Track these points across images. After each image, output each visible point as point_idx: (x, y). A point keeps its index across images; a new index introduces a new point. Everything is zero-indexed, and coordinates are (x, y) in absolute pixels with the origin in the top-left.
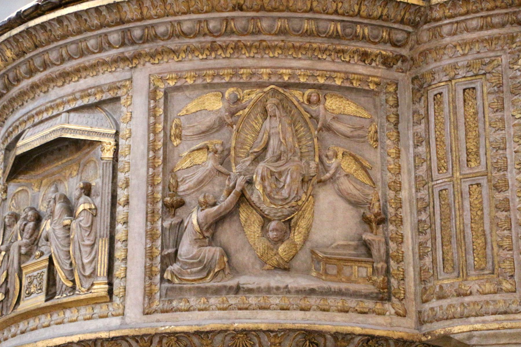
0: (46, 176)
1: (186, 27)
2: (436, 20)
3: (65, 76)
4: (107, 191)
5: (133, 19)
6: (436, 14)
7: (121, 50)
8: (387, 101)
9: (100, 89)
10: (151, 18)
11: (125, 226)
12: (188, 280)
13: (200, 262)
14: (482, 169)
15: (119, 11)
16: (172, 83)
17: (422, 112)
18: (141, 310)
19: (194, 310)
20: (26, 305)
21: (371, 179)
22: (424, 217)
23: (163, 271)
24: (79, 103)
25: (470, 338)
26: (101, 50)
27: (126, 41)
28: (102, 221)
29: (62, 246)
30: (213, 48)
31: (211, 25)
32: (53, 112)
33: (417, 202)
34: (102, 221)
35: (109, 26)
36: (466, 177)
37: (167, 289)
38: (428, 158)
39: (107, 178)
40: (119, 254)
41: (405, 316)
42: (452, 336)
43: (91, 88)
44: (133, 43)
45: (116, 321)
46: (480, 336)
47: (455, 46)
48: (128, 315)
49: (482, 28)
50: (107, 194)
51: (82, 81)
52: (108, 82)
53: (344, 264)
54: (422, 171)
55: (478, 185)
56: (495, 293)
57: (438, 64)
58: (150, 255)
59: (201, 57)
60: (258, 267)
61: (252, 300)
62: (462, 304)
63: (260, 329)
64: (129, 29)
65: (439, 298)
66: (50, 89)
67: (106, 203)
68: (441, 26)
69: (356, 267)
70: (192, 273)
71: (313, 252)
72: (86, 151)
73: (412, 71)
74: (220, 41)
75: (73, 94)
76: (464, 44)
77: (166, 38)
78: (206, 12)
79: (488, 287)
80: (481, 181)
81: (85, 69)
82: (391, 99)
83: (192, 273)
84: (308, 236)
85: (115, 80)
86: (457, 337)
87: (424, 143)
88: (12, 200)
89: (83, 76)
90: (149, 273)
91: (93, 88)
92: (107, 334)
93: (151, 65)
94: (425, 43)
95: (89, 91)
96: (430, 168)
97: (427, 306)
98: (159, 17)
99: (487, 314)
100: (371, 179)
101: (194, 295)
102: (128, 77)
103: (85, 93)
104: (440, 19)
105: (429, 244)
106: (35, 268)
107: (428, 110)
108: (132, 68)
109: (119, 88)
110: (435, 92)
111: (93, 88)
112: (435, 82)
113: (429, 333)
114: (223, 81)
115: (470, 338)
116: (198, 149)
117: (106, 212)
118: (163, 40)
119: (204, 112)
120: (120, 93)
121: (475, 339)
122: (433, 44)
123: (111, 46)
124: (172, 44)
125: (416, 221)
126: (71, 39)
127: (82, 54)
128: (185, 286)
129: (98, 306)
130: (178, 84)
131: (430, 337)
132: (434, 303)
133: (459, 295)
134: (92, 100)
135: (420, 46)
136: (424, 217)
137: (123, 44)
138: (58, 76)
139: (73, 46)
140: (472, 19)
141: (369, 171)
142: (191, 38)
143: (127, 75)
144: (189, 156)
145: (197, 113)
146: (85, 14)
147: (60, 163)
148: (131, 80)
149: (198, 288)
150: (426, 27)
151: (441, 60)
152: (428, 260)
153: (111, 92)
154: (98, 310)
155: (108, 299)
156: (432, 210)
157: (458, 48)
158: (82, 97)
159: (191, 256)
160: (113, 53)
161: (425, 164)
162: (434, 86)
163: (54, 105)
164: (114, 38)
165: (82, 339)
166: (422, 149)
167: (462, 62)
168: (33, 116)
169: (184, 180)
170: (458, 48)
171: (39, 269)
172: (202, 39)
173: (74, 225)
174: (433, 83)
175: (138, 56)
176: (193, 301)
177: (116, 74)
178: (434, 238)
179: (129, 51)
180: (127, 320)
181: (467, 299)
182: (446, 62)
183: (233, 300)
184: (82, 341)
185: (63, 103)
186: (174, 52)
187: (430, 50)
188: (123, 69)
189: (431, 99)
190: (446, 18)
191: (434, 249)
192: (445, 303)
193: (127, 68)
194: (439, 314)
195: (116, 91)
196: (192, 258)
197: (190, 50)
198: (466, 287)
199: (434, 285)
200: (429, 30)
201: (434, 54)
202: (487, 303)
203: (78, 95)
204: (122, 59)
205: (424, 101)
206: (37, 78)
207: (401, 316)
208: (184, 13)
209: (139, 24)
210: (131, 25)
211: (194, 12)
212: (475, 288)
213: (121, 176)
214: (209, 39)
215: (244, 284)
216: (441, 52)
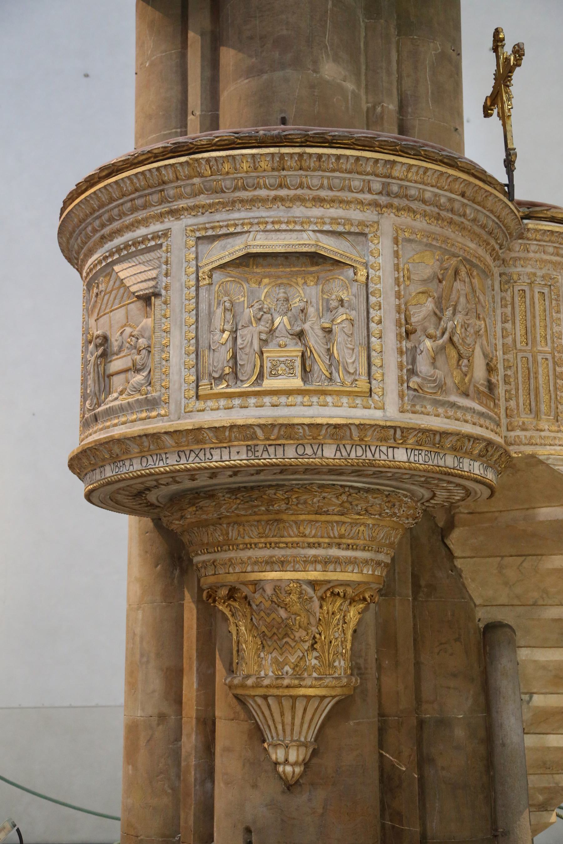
0: (269, 276)
1: (427, 195)
2: (528, 239)
3: (319, 201)
4: (362, 308)
5: (381, 174)
6: (530, 235)
7: (376, 197)
9: (349, 221)
10: (411, 181)
11: (379, 340)
12: (427, 392)
13: (435, 381)
14: (548, 349)
15: (392, 168)
17: (509, 299)
18: (398, 409)
19: (432, 415)
20: (269, 384)
22: (509, 373)
23: (408, 382)
24: (326, 228)
25: (548, 459)
26: (362, 191)
27: (384, 192)
28: (360, 332)
29: (323, 343)
30: (438, 217)
31: (443, 200)
32: (294, 226)
33: (504, 361)
34: (360, 332)
35: (377, 176)
36: (540, 352)
37: (415, 396)
38: (514, 333)
39: (362, 298)
40: (376, 360)
42: (537, 456)
43: (341, 218)
44: (388, 195)
45: (378, 414)
46: (554, 459)
47: (536, 261)
48: (388, 410)
49: (552, 254)
50: (362, 311)
51: (332, 210)
52: (358, 218)
54: (509, 340)
55: (547, 359)
56: (557, 432)
57: (523, 269)
58: (401, 367)
59: (428, 221)
60: (455, 390)
61: (459, 414)
62: (540, 436)
64: (389, 184)
65: (523, 430)
66: (294, 206)
67: (363, 318)
68: (529, 244)
70: (430, 387)
71: (475, 386)
72: (328, 268)
73: (500, 268)
74: (443, 214)
75: (322, 218)
76: (542, 261)
77: (411, 199)
78: (445, 190)
79: (554, 428)
80: (548, 357)
81: (341, 202)
83: (430, 387)
85: (364, 219)
86: (541, 458)
87: (510, 322)
88: (219, 286)
89: (335, 207)
90: (401, 381)
91: (343, 219)
92: (384, 423)
93: (394, 216)
94: (515, 252)
95: (339, 220)
96: (514, 341)
97: (512, 434)
98: (416, 182)
99: (556, 445)
101: (430, 404)
102: (376, 220)
103: (334, 220)
104: (531, 240)
105: (513, 392)
106: (288, 354)
107: (513, 300)
108: (379, 214)
109: (368, 227)
110: (519, 289)
111: (343, 219)
112: (520, 281)
113: (520, 452)
114: (438, 245)
115: (548, 459)
116: (423, 293)
117: (363, 325)
118: (408, 200)
119: (423, 264)
120: (367, 230)
121: (551, 460)
122: (522, 255)
123: (370, 191)
124: (414, 205)
125: (503, 375)
126: (337, 174)
127: (342, 189)
128: (428, 396)
129: (359, 398)
130: (411, 237)
131: (520, 455)
132: (518, 433)
133: (537, 430)
134: (340, 229)
135: (511, 253)
136: (509, 373)
137: (380, 193)
138: (311, 199)
139: (337, 181)
140: (549, 246)
142: (426, 205)
143: (375, 218)
144: (416, 296)
145: (420, 264)
146: (365, 161)
147: (288, 270)
148: (378, 223)
149: (435, 399)
150: (520, 241)
151: (526, 267)
152: (512, 403)
153: (360, 228)
154: (358, 401)
155: (369, 394)
156: (516, 369)
157: (538, 263)
158: (331, 224)
159: (430, 374)
160: (368, 197)
161: (511, 336)
162: (519, 284)
163: (298, 221)
164: (376, 186)
165: (362, 422)
166: (509, 326)
167: (540, 273)
168: (267, 223)
169: (414, 314)
170: (538, 263)
171: (287, 356)
172: (433, 209)
173: (336, 329)
174: (518, 281)
175: (390, 206)
176: (429, 408)
177: (366, 214)
178: (517, 389)
179: (383, 200)
180: (388, 414)
181: (543, 434)
182: (529, 269)
183: (451, 413)
184: (362, 425)
185: (310, 222)
186: (414, 212)
187: (520, 259)
188: (372, 212)
189: (516, 292)
190: (536, 240)
191: (517, 397)
192: (528, 434)
193: (375, 212)
194: (524, 441)
195: (364, 228)
196: (430, 376)
197: (425, 214)
198: (540, 427)
199: (517, 421)
200: (521, 244)
201: (522, 262)
202: (555, 438)
203: (327, 221)
204: (375, 204)
205: (511, 293)
206: (283, 192)
208: (432, 186)
209: (399, 182)
210: (394, 181)
211: (438, 188)
212: (546, 427)
213: (372, 299)
214: (436, 210)
216: (527, 262)
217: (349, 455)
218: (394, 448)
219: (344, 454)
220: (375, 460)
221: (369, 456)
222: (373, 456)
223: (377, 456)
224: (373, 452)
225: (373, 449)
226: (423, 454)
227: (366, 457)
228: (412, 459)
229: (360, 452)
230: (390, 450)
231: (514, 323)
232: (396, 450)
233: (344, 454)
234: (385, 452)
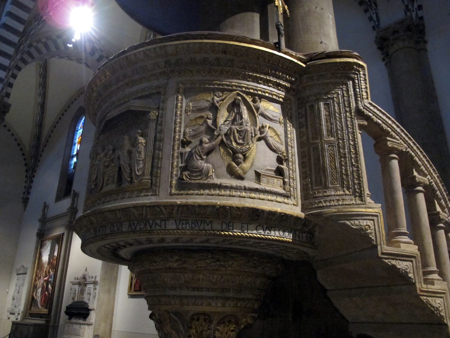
8: (287, 107)
16: (188, 86)
17: (304, 113)
21: (281, 141)
24: (140, 95)
41: (297, 206)
53: (271, 178)
63: (232, 206)
69: (276, 180)
82: (288, 106)
84: (253, 163)
96: (308, 138)
100: (281, 141)
105: (308, 173)
141: (280, 137)
166: (304, 129)
178: (310, 170)
189: (308, 107)
207: (295, 206)
215: (223, 183)
217: (136, 229)
218: (165, 220)
219: (133, 228)
220: (152, 230)
221: (148, 227)
222: (151, 227)
223: (153, 227)
224: (151, 224)
225: (151, 222)
226: (190, 223)
227: (146, 228)
228: (180, 227)
229: (142, 226)
230: (163, 223)
231: (307, 128)
232: (167, 222)
233: (133, 228)
234: (159, 224)
